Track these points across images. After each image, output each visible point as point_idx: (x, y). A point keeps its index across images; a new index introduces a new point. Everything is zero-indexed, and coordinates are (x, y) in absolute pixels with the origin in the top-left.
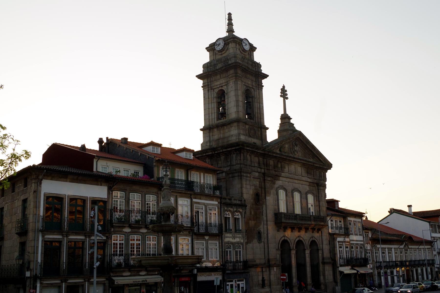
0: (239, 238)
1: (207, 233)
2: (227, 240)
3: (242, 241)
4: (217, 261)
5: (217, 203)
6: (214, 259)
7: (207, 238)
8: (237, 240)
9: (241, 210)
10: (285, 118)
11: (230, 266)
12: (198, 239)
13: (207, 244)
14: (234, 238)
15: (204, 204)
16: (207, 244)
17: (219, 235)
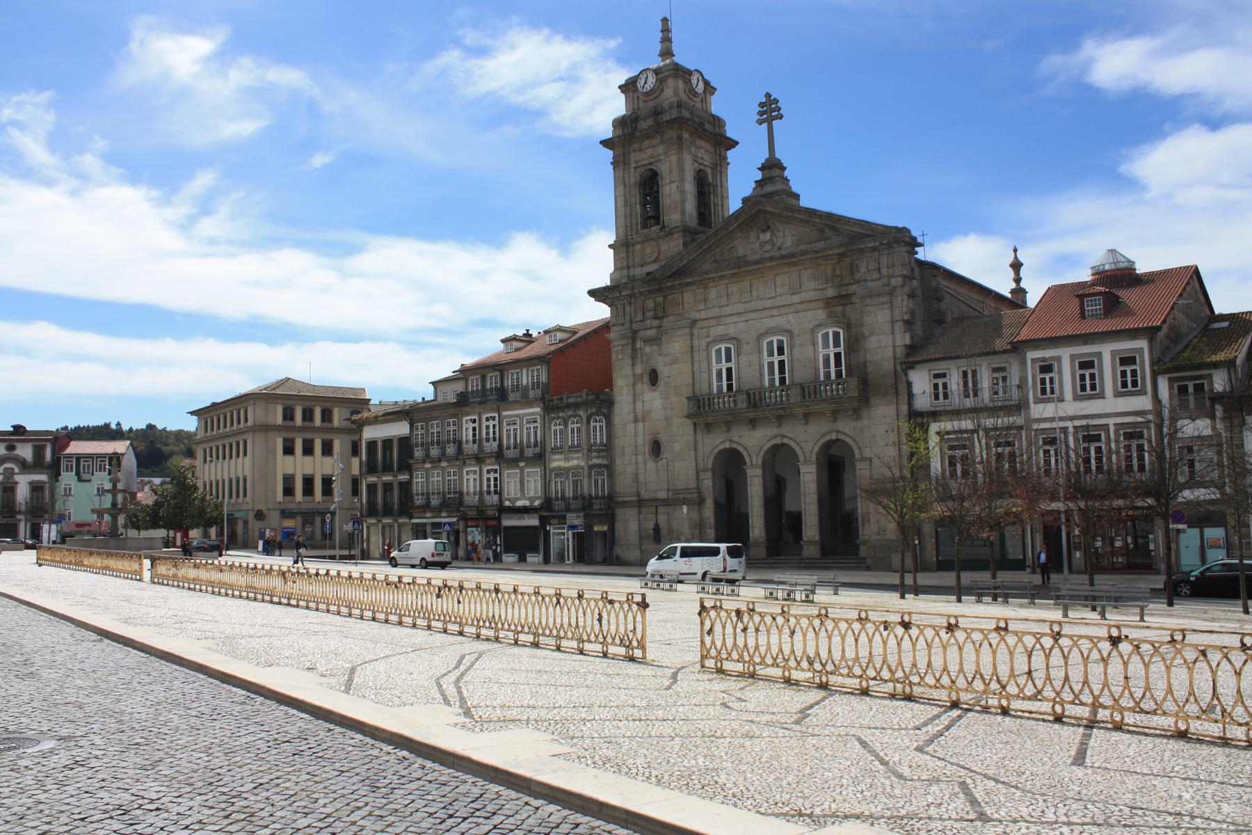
0: (578, 458)
1: (522, 457)
2: (554, 465)
3: (583, 464)
4: (538, 498)
5: (538, 410)
6: (532, 494)
7: (522, 464)
8: (575, 462)
9: (581, 413)
10: (773, 168)
11: (558, 505)
12: (508, 468)
13: (522, 473)
14: (567, 459)
15: (518, 416)
16: (522, 473)
17: (540, 459)
